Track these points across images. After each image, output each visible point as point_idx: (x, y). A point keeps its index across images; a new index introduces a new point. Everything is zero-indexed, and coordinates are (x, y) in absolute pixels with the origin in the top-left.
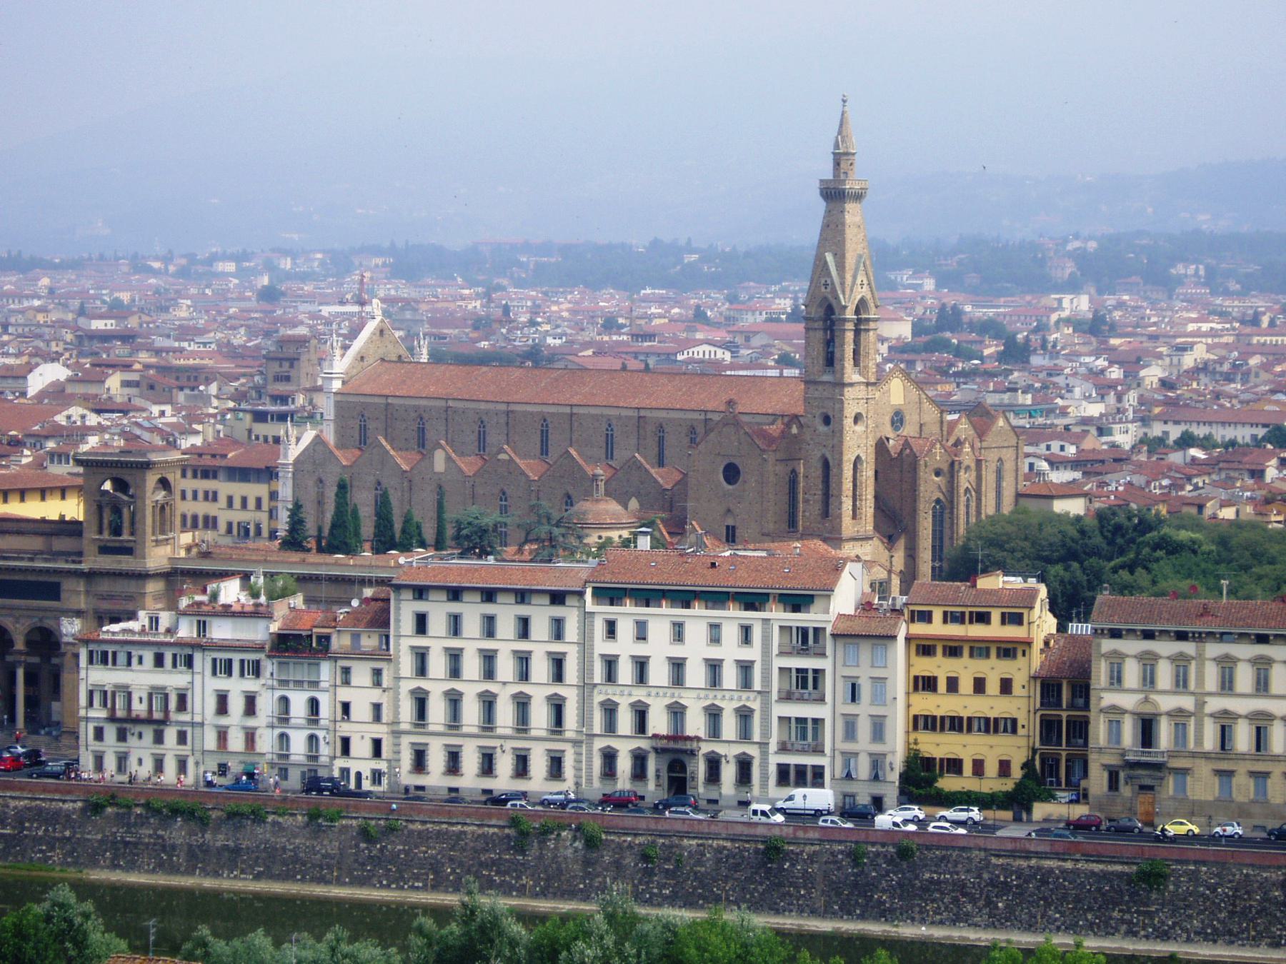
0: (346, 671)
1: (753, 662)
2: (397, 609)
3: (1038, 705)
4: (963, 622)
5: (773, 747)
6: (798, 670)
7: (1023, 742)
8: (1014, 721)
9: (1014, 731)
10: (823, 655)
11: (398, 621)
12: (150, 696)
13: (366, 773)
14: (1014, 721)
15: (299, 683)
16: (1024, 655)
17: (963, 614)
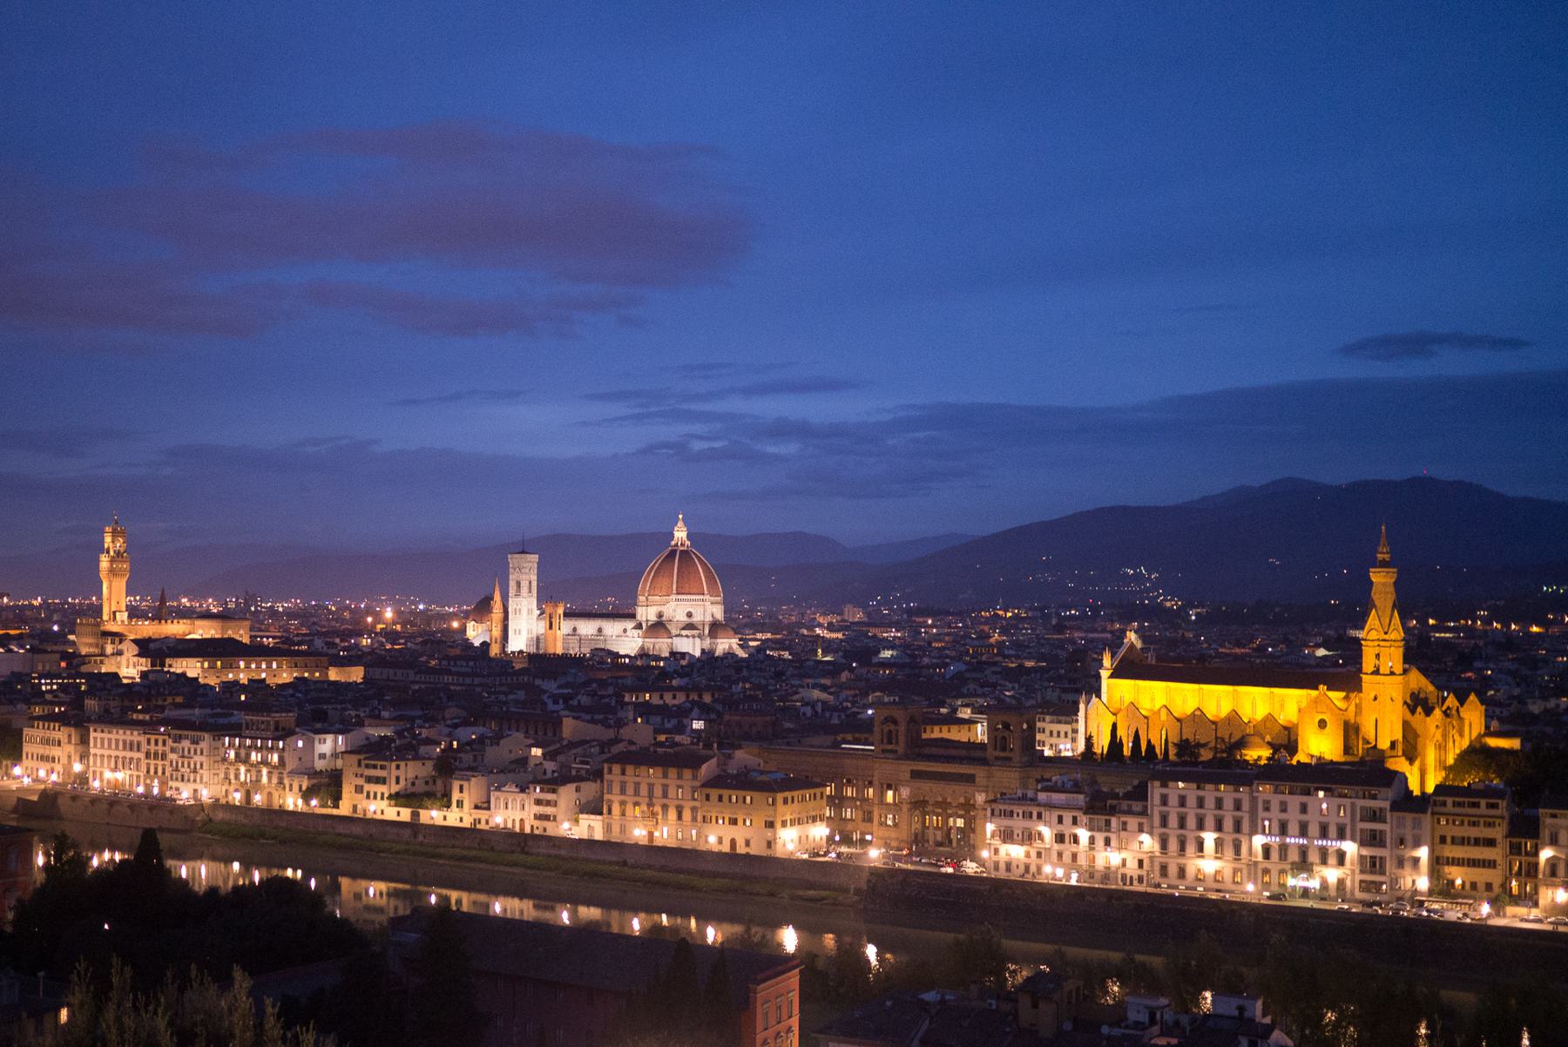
0: (1125, 824)
1: (1345, 825)
2: (1152, 792)
3: (1508, 853)
4: (1464, 806)
5: (1357, 871)
6: (1371, 830)
7: (1500, 872)
8: (1495, 861)
9: (1495, 867)
10: (1385, 822)
11: (1152, 798)
12: (1023, 833)
13: (1135, 877)
14: (1495, 861)
15: (1100, 830)
16: (1499, 825)
17: (1464, 802)
